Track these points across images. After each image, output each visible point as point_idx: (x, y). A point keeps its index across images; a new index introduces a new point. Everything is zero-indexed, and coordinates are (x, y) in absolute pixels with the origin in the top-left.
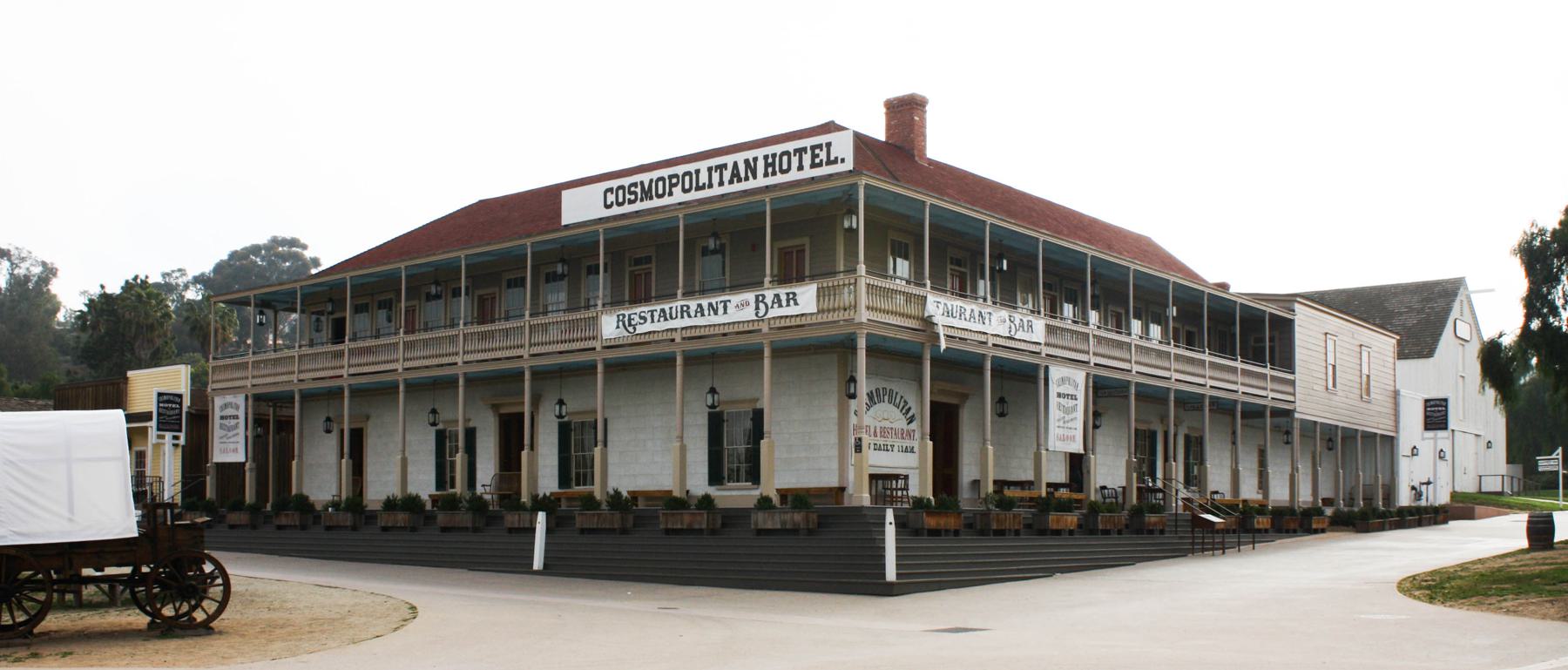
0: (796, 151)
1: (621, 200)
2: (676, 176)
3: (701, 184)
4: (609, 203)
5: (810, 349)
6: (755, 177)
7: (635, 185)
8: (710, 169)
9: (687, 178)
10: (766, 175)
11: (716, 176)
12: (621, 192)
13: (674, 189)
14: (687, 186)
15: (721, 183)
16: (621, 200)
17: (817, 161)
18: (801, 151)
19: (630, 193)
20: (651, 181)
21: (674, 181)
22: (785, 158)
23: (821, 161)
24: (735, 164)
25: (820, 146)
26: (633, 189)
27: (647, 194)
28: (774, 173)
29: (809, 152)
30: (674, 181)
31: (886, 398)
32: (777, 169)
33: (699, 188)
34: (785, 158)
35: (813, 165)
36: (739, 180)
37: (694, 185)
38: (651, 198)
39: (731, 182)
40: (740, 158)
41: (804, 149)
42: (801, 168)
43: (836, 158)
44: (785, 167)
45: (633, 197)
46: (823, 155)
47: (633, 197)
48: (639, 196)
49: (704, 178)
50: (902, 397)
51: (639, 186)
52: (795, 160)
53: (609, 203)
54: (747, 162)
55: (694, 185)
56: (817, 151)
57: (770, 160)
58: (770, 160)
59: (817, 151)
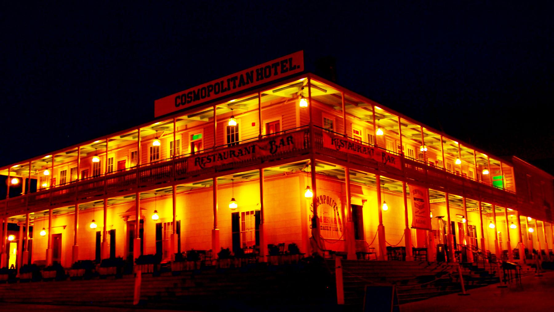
0: (273, 65)
1: (184, 102)
2: (211, 86)
3: (224, 89)
4: (178, 103)
5: (284, 174)
6: (252, 81)
7: (190, 93)
8: (229, 81)
9: (217, 86)
10: (258, 80)
11: (232, 84)
12: (184, 97)
13: (210, 93)
14: (217, 90)
15: (234, 87)
16: (184, 102)
17: (285, 69)
18: (276, 65)
19: (189, 97)
20: (199, 90)
21: (211, 88)
22: (268, 70)
23: (287, 69)
24: (242, 76)
25: (286, 61)
26: (190, 95)
27: (197, 97)
28: (262, 78)
29: (280, 64)
30: (211, 88)
31: (326, 201)
32: (264, 76)
33: (223, 91)
34: (268, 70)
35: (283, 71)
36: (244, 84)
37: (221, 90)
38: (199, 99)
39: (240, 86)
40: (244, 72)
41: (277, 64)
42: (276, 73)
43: (295, 66)
44: (268, 74)
45: (190, 99)
46: (288, 65)
47: (190, 99)
48: (193, 99)
49: (225, 85)
50: (333, 201)
51: (193, 94)
52: (273, 70)
53: (178, 103)
54: (247, 74)
55: (221, 90)
56: (285, 64)
57: (260, 72)
58: (260, 72)
59: (285, 64)
